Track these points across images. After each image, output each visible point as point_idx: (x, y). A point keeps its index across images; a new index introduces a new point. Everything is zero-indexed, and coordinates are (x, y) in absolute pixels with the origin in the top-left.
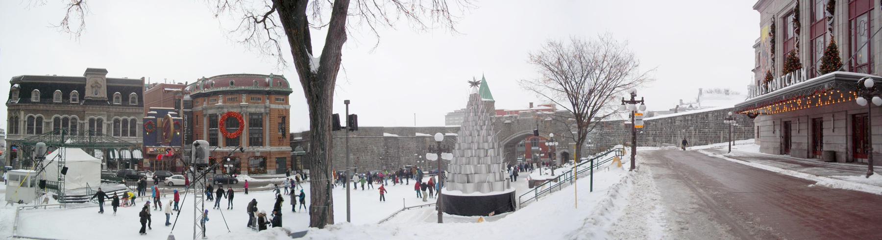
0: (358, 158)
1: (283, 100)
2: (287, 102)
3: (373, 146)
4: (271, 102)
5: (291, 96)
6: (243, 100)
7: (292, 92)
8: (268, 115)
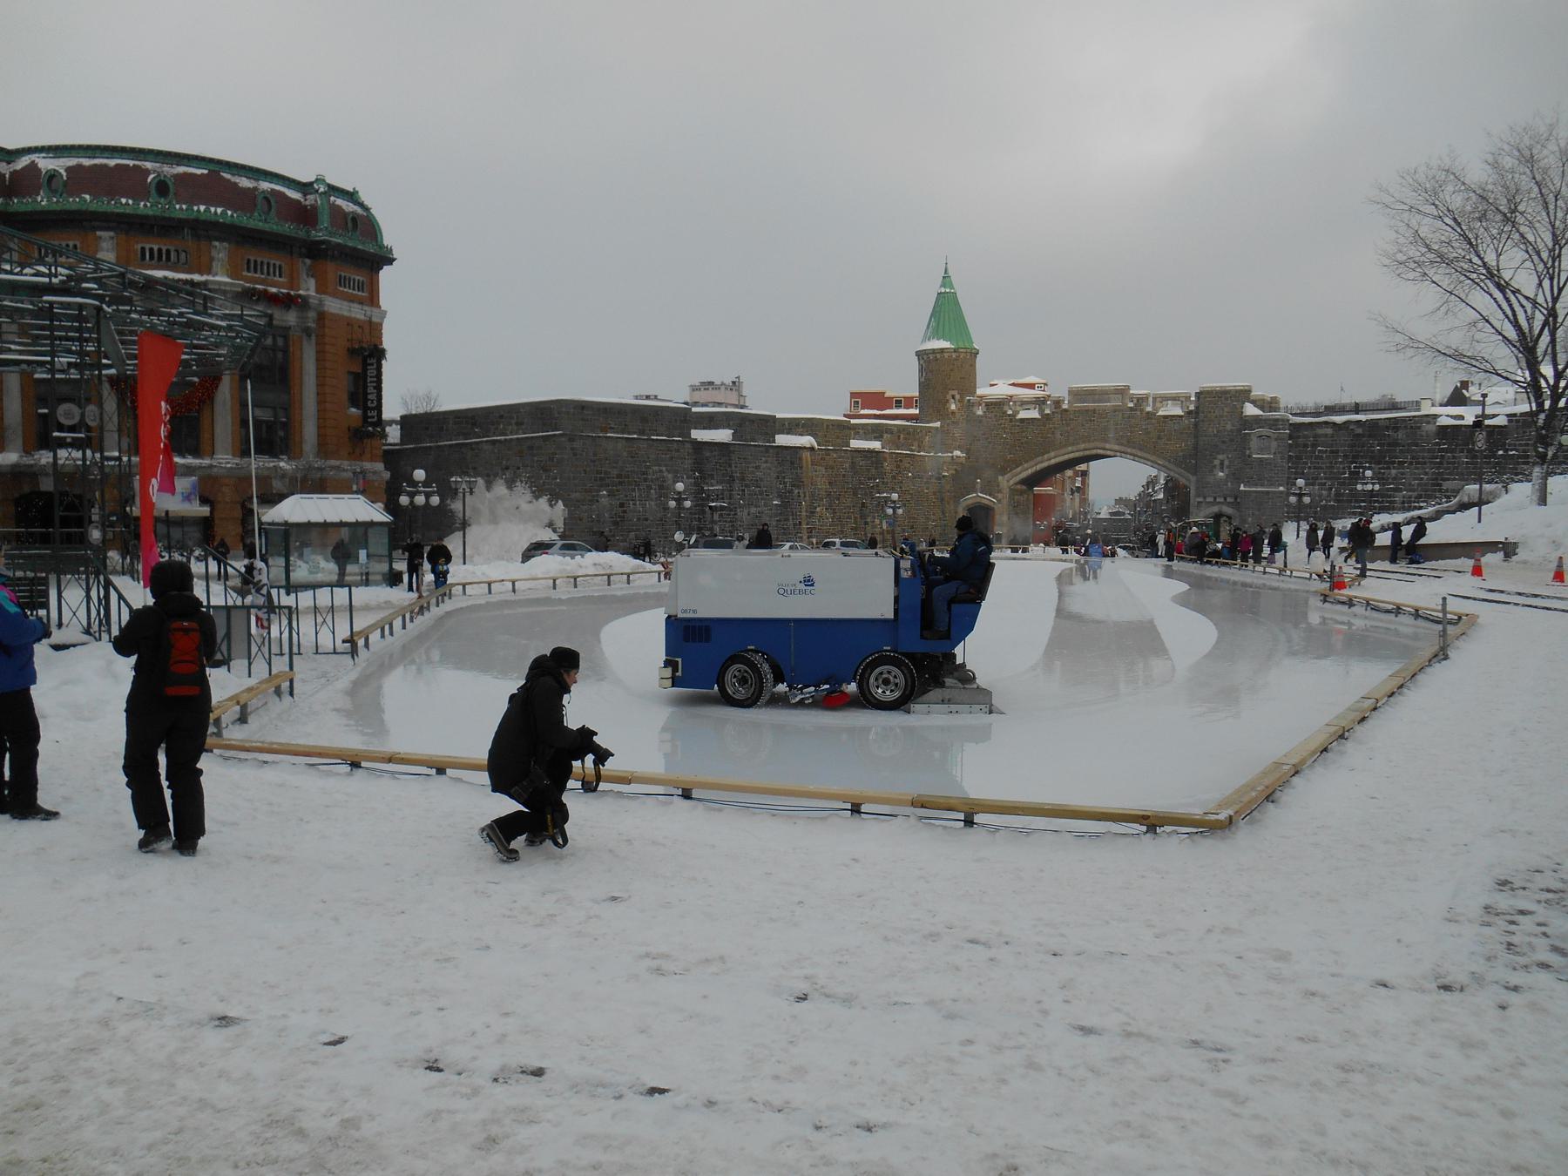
0: (622, 505)
1: (361, 287)
2: (373, 299)
3: (664, 469)
4: (321, 289)
5: (386, 274)
6: (216, 266)
7: (390, 261)
8: (313, 338)
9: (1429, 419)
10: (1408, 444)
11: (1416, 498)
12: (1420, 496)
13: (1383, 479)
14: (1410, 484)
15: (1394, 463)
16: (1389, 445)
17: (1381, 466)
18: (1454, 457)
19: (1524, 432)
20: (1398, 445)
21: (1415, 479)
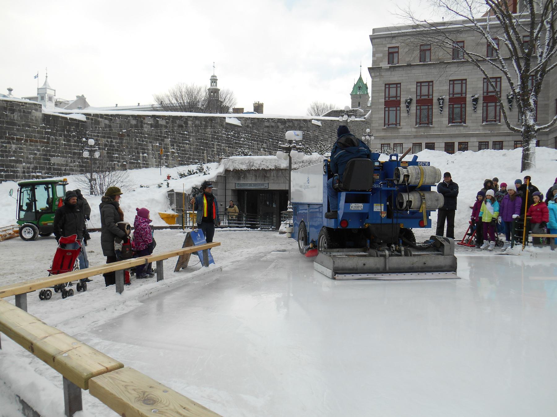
9: (37, 107)
10: (23, 125)
11: (33, 169)
12: (35, 168)
13: (6, 151)
14: (27, 158)
15: (13, 139)
16: (7, 123)
17: (3, 140)
18: (56, 139)
19: (96, 128)
20: (14, 124)
21: (30, 154)
